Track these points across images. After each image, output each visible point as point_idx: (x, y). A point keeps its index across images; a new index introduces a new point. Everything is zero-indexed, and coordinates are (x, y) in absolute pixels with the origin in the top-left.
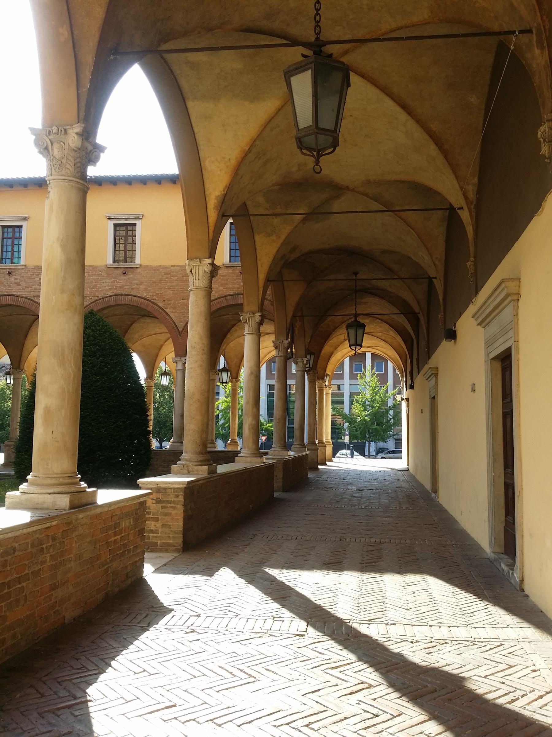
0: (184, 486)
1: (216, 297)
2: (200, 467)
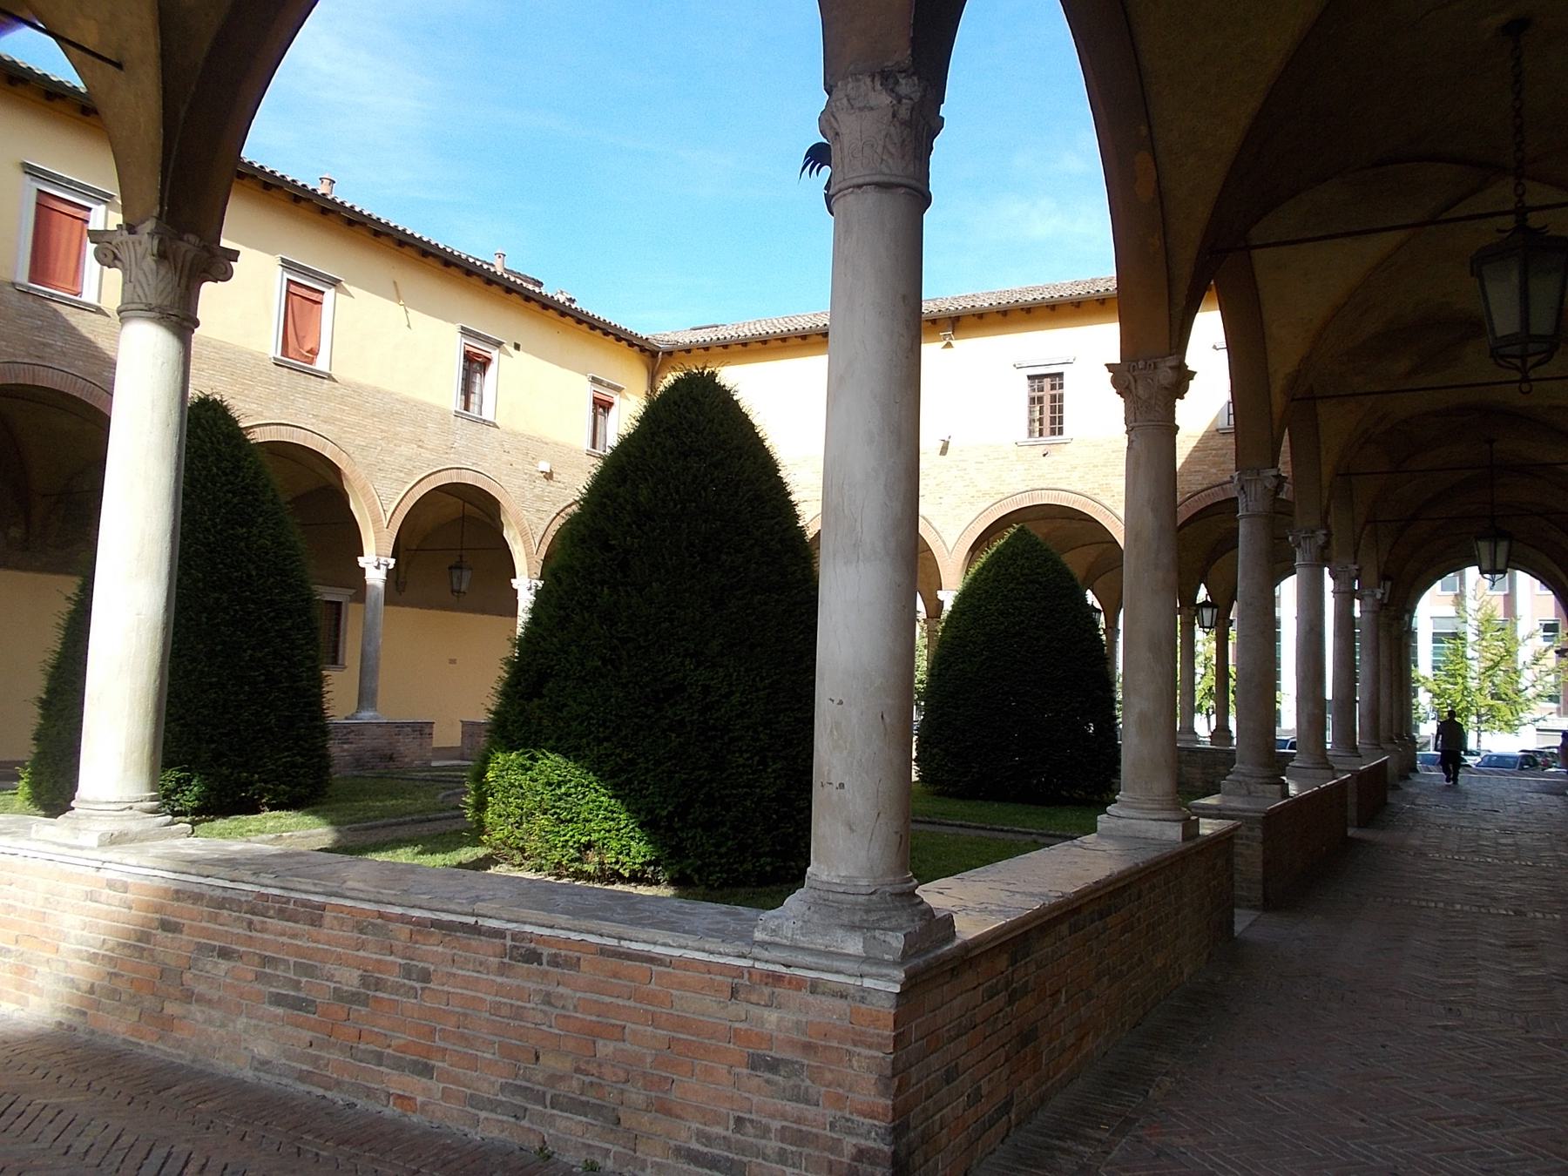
0: (1263, 815)
1: (1205, 486)
2: (1268, 787)
